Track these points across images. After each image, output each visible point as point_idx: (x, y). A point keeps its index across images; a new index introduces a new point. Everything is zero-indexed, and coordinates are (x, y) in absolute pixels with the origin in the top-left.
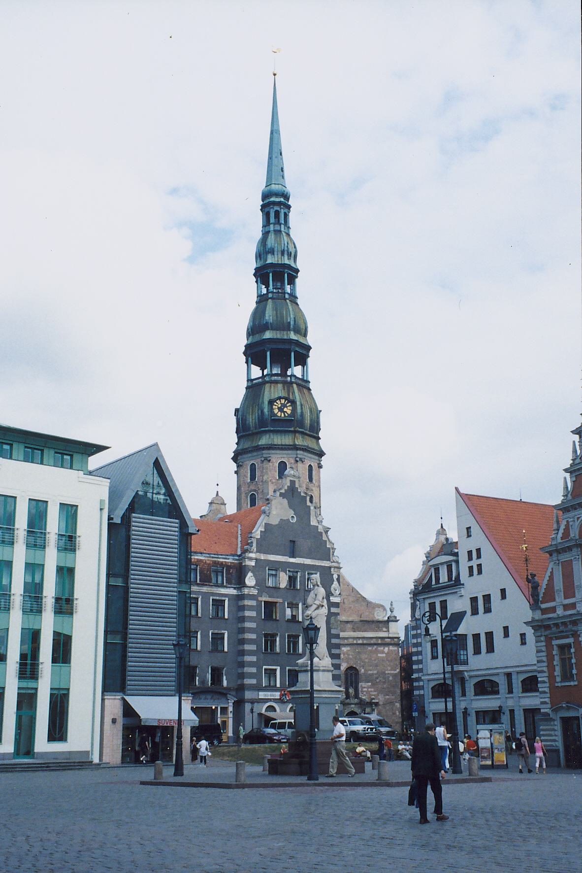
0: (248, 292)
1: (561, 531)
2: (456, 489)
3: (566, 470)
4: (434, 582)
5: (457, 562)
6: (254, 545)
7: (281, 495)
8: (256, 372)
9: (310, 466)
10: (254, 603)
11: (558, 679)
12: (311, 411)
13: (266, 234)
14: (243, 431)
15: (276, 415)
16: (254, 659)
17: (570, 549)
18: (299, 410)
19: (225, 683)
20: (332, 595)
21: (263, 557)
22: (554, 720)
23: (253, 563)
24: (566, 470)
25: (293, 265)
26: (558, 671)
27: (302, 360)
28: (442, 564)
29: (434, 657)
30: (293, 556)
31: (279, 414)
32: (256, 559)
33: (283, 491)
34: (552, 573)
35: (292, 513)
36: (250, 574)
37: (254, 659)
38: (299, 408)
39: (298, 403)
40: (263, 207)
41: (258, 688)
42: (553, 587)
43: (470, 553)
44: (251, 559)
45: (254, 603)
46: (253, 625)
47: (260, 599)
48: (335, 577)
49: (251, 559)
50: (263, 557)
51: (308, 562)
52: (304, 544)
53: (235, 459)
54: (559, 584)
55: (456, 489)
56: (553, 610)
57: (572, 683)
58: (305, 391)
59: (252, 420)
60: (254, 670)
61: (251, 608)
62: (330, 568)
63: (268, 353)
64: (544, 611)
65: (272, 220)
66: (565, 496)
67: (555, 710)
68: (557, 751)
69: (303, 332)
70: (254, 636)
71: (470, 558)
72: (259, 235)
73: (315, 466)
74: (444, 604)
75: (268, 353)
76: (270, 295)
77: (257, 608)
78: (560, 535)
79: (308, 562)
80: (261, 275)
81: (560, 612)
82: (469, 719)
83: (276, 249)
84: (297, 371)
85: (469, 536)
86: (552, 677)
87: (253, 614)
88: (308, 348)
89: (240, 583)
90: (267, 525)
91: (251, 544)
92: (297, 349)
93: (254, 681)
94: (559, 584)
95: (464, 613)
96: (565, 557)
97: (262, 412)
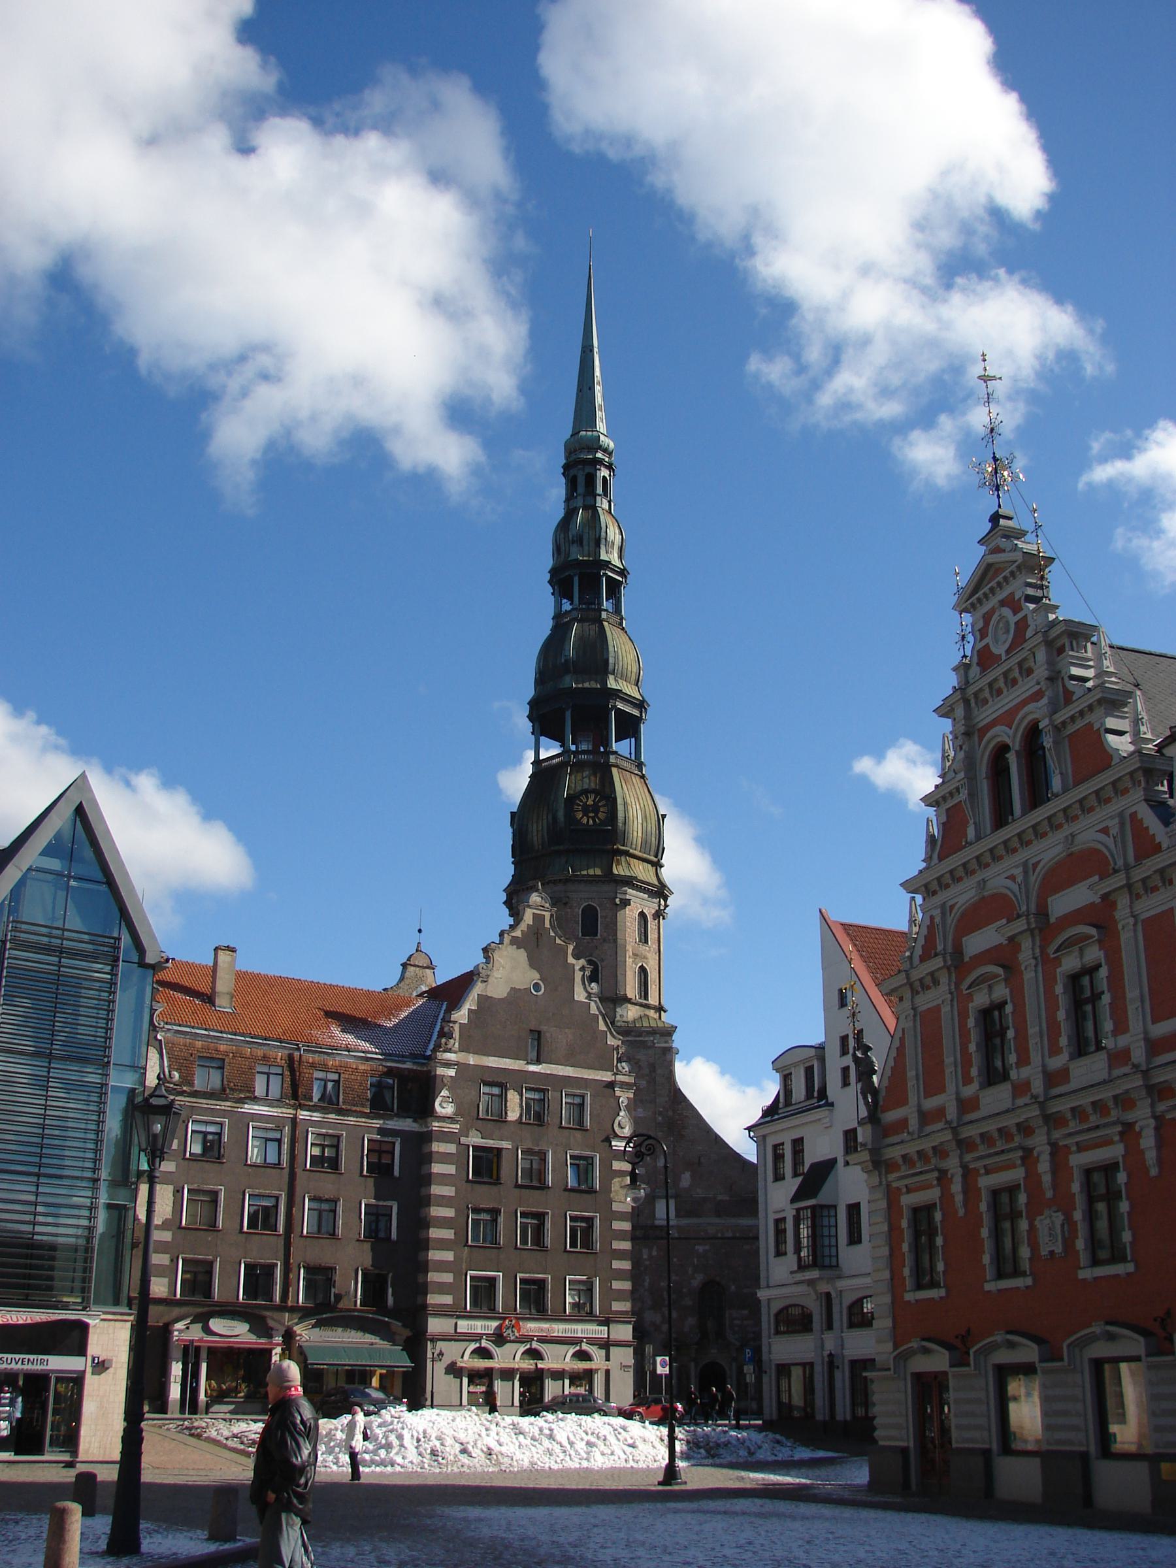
0: (537, 611)
4: (781, 1105)
5: (822, 1060)
6: (456, 1035)
7: (515, 942)
8: (550, 750)
9: (642, 915)
10: (451, 1148)
11: (909, 1283)
12: (645, 817)
13: (570, 514)
14: (521, 850)
15: (579, 822)
16: (449, 1256)
18: (620, 814)
19: (390, 1301)
20: (616, 1136)
21: (472, 1060)
23: (452, 1072)
25: (615, 561)
27: (630, 727)
28: (796, 1065)
29: (779, 1253)
30: (538, 1061)
31: (585, 820)
32: (457, 1064)
33: (518, 933)
35: (535, 976)
36: (444, 1093)
37: (449, 1256)
38: (620, 808)
39: (619, 801)
40: (567, 468)
41: (455, 1312)
43: (844, 1039)
44: (448, 1064)
45: (451, 1148)
46: (448, 1191)
47: (463, 1140)
48: (623, 1101)
49: (448, 1064)
50: (472, 1060)
51: (569, 1071)
52: (559, 1037)
53: (508, 903)
58: (636, 780)
59: (537, 831)
60: (448, 1278)
61: (445, 1158)
62: (611, 1085)
63: (568, 714)
65: (581, 489)
69: (634, 677)
70: (449, 1213)
71: (844, 1052)
72: (561, 514)
73: (649, 913)
74: (798, 1144)
75: (568, 714)
76: (574, 614)
77: (459, 1160)
79: (569, 1071)
80: (561, 581)
82: (838, 1374)
83: (585, 537)
84: (622, 747)
85: (843, 1004)
87: (451, 1169)
88: (641, 705)
89: (425, 1110)
90: (483, 999)
91: (450, 1036)
92: (620, 706)
93: (448, 1299)
95: (832, 1163)
96: (926, 1000)
97: (555, 819)
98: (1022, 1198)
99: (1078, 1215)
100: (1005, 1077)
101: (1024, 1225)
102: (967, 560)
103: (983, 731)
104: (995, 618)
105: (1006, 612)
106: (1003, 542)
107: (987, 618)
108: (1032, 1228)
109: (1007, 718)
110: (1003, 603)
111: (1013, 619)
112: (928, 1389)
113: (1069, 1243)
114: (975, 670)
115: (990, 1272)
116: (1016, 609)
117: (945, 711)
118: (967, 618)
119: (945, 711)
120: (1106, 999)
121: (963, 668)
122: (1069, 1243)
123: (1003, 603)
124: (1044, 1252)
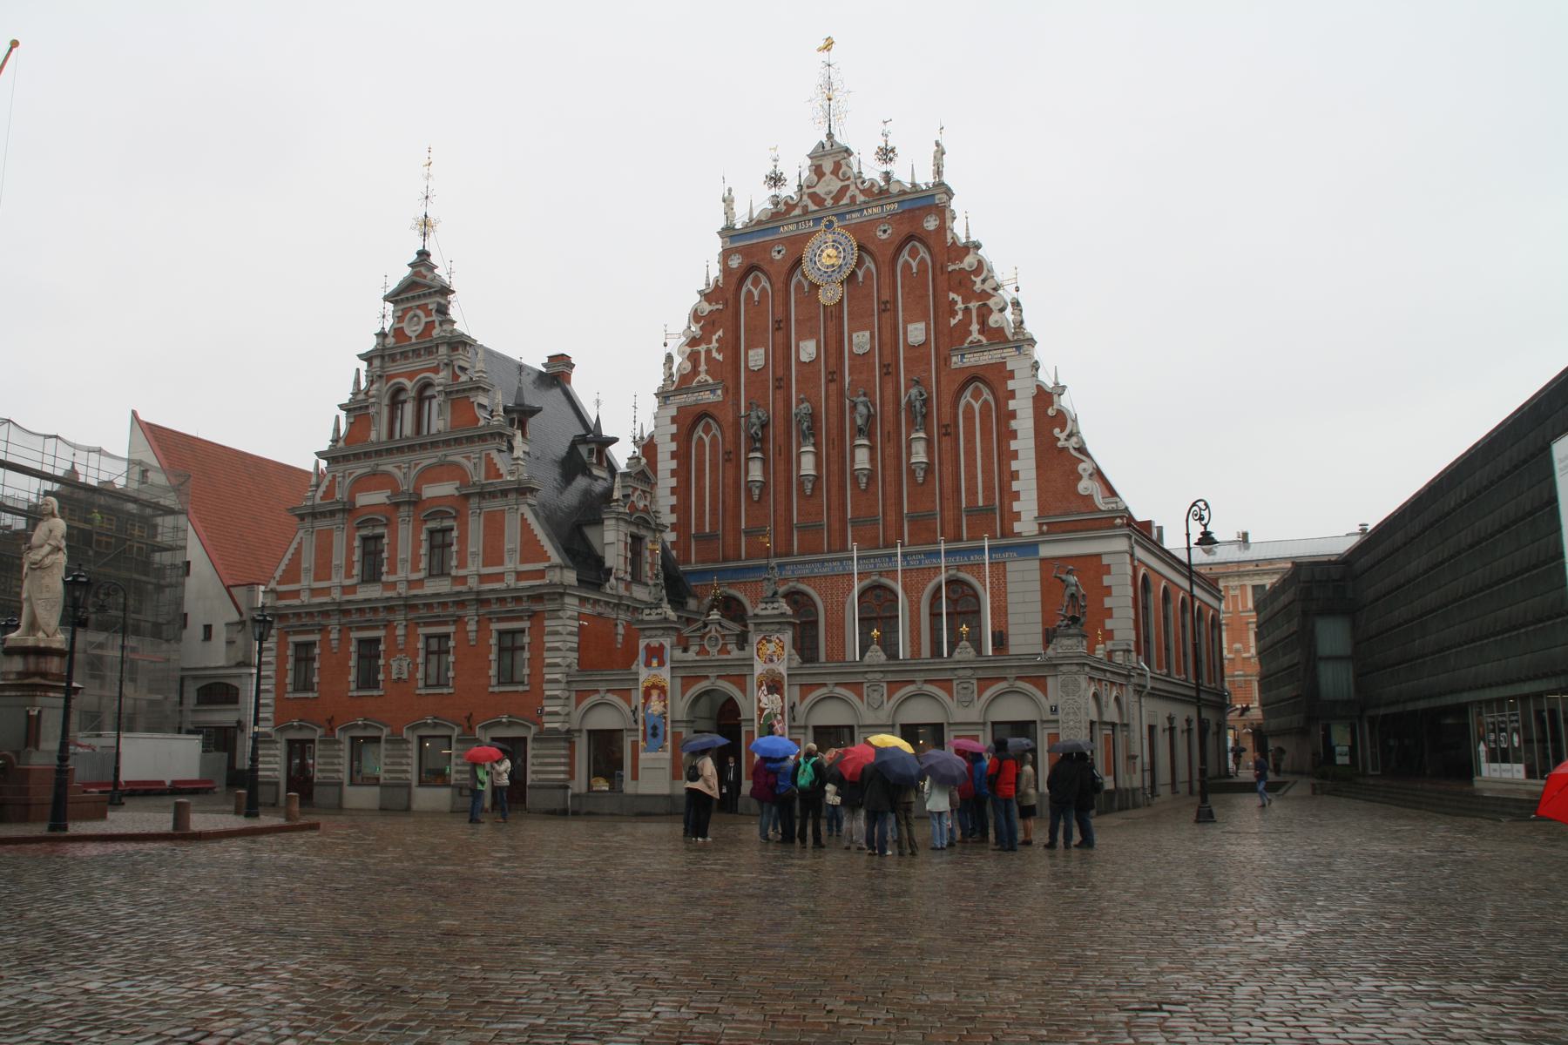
1: (323, 488)
2: (134, 413)
3: (342, 407)
11: (290, 688)
17: (332, 513)
22: (275, 742)
24: (342, 407)
26: (289, 679)
34: (300, 544)
42: (299, 564)
54: (308, 560)
55: (134, 413)
56: (296, 594)
57: (310, 695)
64: (281, 595)
66: (335, 440)
67: (281, 730)
68: (277, 784)
78: (320, 493)
81: (305, 598)
86: (280, 685)
94: (308, 560)
98: (382, 647)
99: (420, 660)
100: (379, 580)
101: (381, 662)
102: (400, 272)
103: (390, 377)
104: (411, 314)
105: (420, 313)
106: (423, 270)
107: (405, 311)
108: (388, 667)
109: (410, 375)
110: (418, 307)
111: (424, 320)
112: (298, 749)
113: (412, 675)
114: (390, 341)
115: (353, 686)
116: (428, 313)
117: (367, 357)
118: (390, 307)
119: (367, 357)
120: (454, 548)
121: (382, 335)
122: (412, 675)
123: (418, 307)
124: (394, 677)
